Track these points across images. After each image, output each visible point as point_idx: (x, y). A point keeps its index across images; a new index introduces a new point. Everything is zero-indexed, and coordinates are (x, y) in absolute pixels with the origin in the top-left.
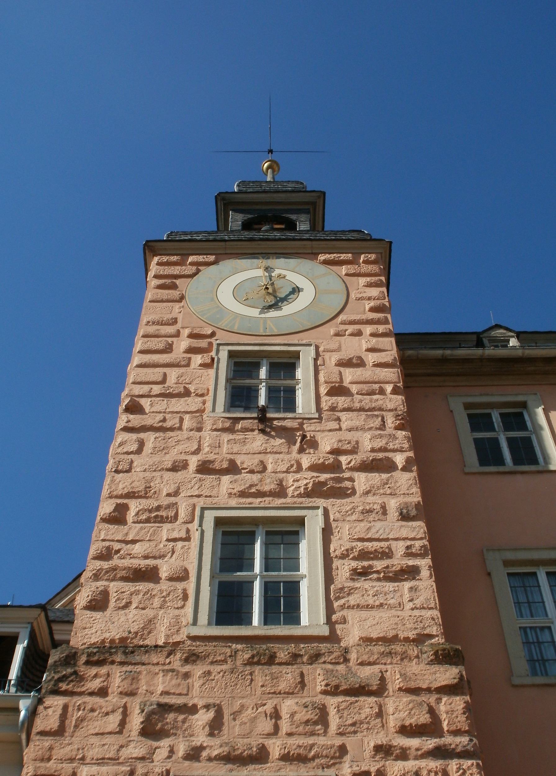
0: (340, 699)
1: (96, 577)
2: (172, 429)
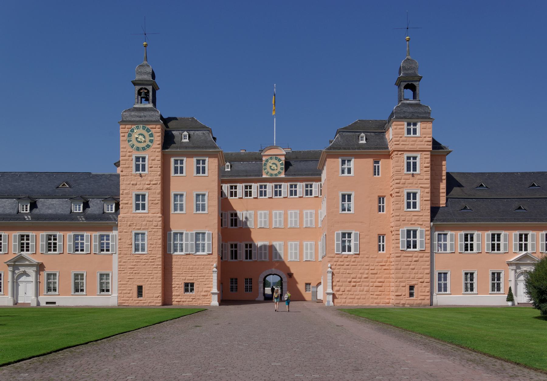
0: (148, 222)
1: (122, 203)
2: (128, 176)
